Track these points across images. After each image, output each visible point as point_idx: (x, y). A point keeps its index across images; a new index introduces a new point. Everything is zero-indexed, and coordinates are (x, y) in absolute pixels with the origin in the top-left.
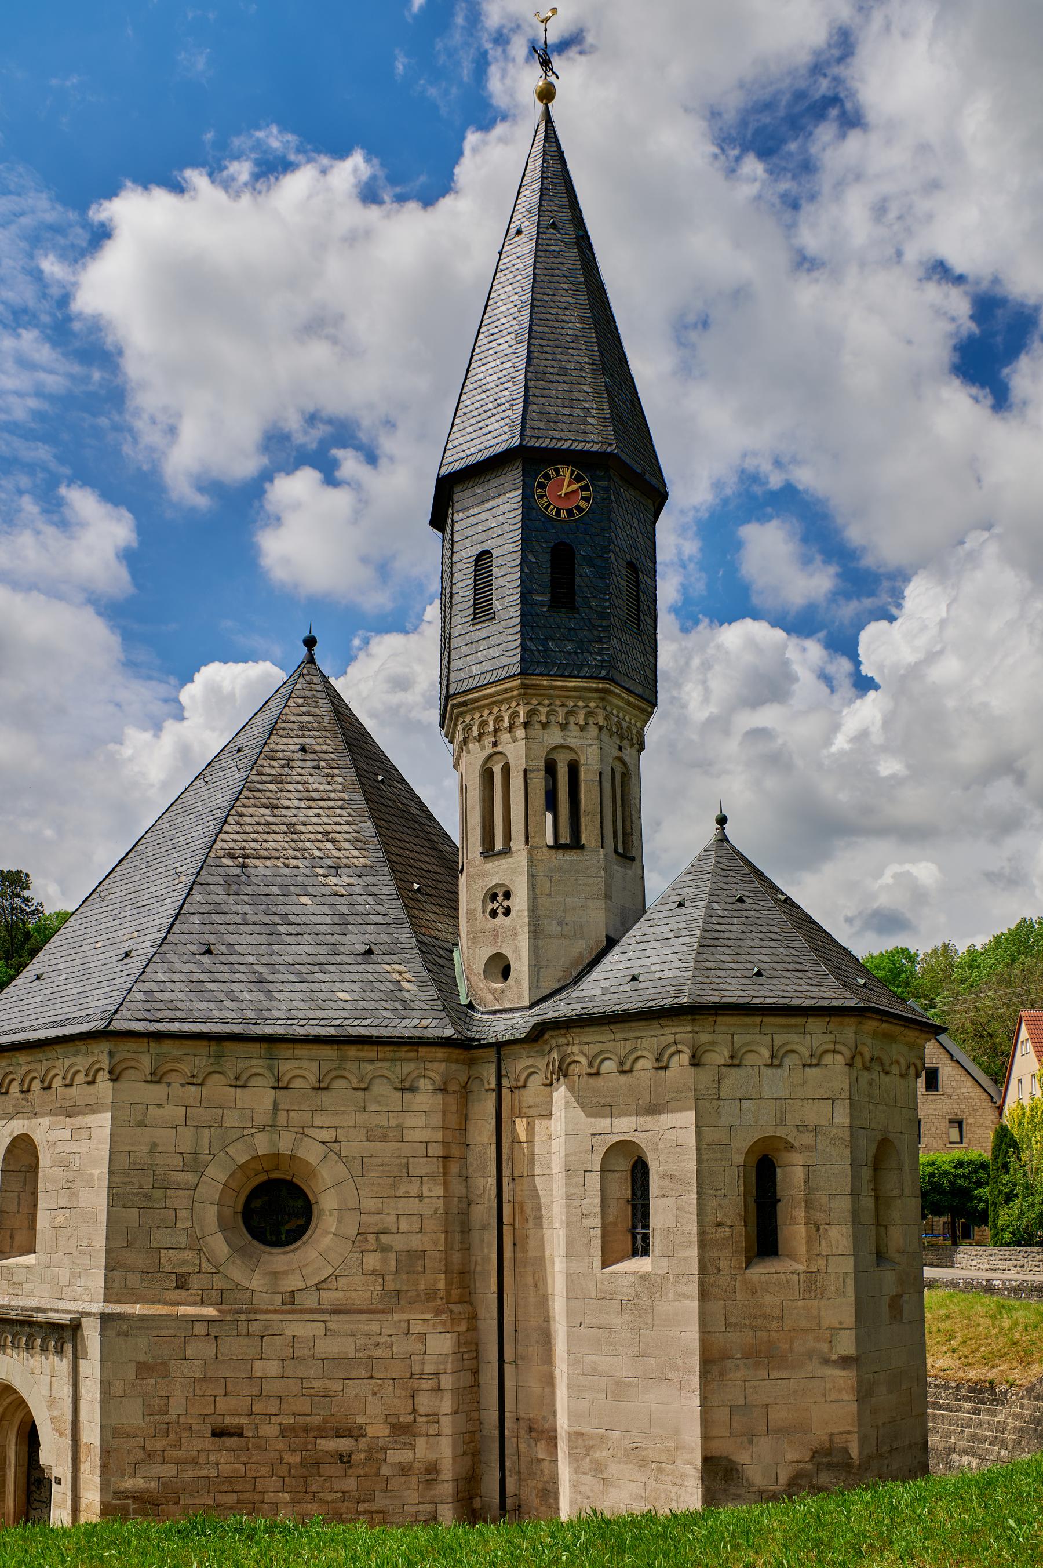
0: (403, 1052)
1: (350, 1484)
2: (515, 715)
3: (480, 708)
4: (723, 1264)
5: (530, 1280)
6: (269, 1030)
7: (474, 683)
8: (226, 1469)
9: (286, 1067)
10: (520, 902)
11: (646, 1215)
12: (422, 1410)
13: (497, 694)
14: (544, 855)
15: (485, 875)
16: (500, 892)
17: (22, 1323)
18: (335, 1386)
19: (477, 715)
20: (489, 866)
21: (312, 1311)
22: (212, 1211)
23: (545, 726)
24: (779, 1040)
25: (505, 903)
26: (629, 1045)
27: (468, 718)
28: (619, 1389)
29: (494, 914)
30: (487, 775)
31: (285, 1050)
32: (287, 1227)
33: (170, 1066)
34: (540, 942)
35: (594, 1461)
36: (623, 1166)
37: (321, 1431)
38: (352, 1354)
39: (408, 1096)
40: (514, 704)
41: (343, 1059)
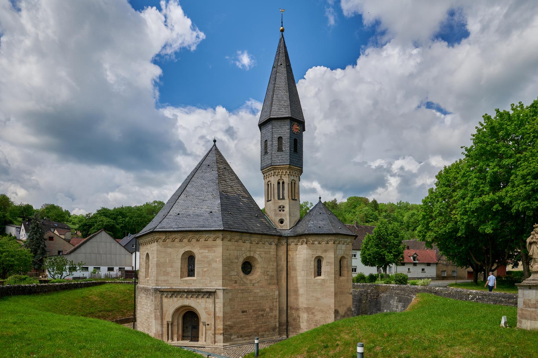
0: (272, 237)
1: (263, 320)
2: (286, 172)
3: (278, 169)
4: (337, 277)
5: (291, 281)
6: (251, 232)
7: (278, 164)
8: (244, 319)
9: (253, 239)
10: (287, 209)
11: (321, 269)
12: (274, 305)
13: (283, 167)
14: (291, 200)
15: (278, 203)
16: (282, 207)
17: (195, 292)
18: (261, 301)
19: (277, 171)
20: (279, 201)
21: (258, 287)
22: (240, 267)
23: (291, 175)
24: (345, 240)
25: (283, 209)
26: (321, 239)
27: (275, 171)
28: (318, 299)
29: (280, 211)
30: (279, 183)
31: (253, 235)
32: (247, 271)
33: (233, 238)
34: (291, 217)
35: (312, 312)
36: (316, 260)
37: (259, 310)
38: (264, 295)
39: (271, 245)
40: (286, 170)
41: (262, 238)
